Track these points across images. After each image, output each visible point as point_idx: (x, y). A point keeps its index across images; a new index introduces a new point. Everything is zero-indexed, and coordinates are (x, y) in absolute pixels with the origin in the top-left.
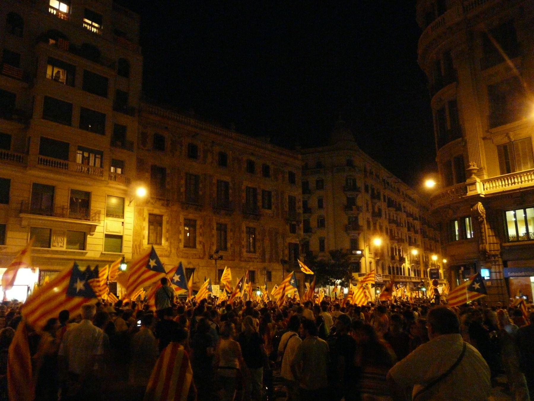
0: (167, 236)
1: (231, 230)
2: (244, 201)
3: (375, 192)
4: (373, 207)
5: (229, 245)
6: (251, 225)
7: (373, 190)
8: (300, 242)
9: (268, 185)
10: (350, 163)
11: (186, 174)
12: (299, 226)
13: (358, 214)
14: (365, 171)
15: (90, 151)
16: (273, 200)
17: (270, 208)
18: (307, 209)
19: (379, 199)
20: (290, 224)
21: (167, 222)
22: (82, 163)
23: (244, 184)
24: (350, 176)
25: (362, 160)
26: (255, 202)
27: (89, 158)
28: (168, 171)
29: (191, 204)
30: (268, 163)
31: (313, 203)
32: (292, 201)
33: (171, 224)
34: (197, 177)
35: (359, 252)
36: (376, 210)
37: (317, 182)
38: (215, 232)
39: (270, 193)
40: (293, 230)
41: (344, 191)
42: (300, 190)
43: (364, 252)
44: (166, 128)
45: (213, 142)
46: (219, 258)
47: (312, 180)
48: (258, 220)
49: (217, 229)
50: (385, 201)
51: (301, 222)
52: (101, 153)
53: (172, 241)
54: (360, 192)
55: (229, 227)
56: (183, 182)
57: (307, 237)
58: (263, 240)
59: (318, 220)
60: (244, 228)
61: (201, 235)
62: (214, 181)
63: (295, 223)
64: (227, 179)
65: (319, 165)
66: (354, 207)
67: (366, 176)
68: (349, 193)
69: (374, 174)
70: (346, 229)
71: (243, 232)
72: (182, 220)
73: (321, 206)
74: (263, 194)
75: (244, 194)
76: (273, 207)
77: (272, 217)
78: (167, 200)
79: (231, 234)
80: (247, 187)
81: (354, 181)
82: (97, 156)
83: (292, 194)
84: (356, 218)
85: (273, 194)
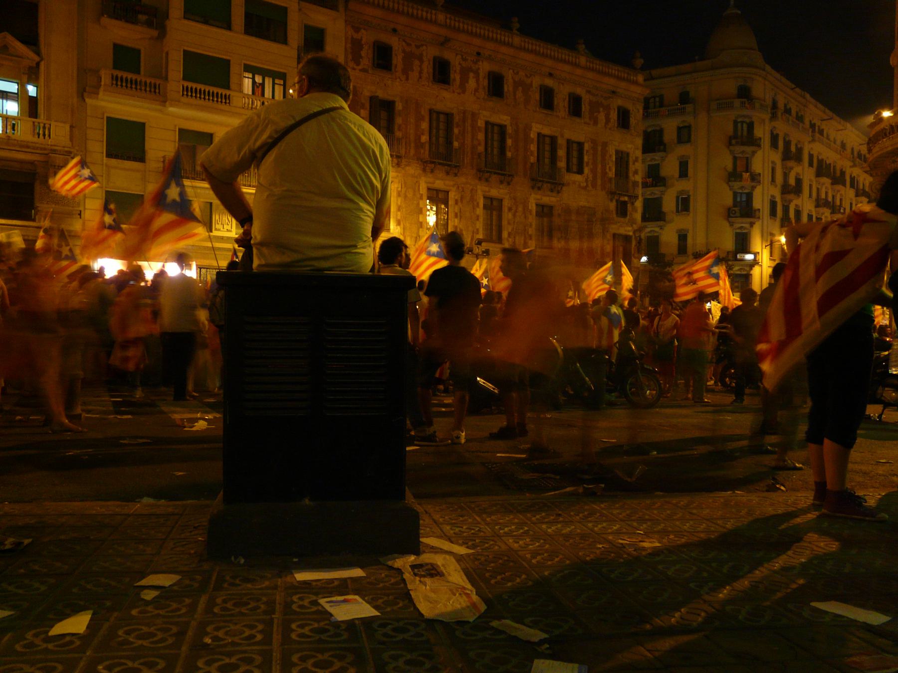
0: (399, 217)
2: (533, 159)
3: (793, 149)
4: (786, 176)
5: (505, 234)
7: (787, 144)
8: (634, 232)
9: (578, 131)
10: (744, 93)
11: (431, 111)
12: (633, 204)
13: (753, 188)
14: (775, 106)
15: (265, 73)
16: (586, 158)
17: (580, 171)
18: (655, 177)
19: (798, 158)
20: (617, 201)
21: (399, 195)
22: (253, 93)
23: (534, 129)
24: (744, 116)
25: (767, 85)
26: (554, 159)
27: (263, 85)
28: (399, 106)
29: (440, 164)
30: (579, 91)
31: (670, 168)
32: (622, 160)
33: (406, 197)
34: (449, 116)
35: (749, 257)
36: (792, 181)
37: (679, 129)
38: (480, 211)
39: (580, 145)
40: (622, 210)
41: (730, 144)
42: (639, 142)
43: (759, 257)
44: (395, 30)
45: (478, 54)
46: (483, 252)
47: (670, 126)
48: (558, 192)
49: (485, 207)
50: (811, 165)
51: (636, 197)
52: (283, 76)
53: (408, 225)
54: (759, 146)
55: (506, 203)
56: (425, 125)
57: (657, 229)
59: (677, 198)
60: (532, 207)
61: (456, 216)
62: (481, 123)
63: (626, 199)
65: (685, 98)
66: (746, 175)
67: (774, 117)
68: (738, 149)
69: (794, 112)
70: (729, 214)
72: (423, 190)
73: (684, 173)
74: (568, 148)
75: (533, 147)
77: (585, 188)
78: (398, 157)
79: (510, 215)
80: (539, 134)
81: (751, 126)
82: (277, 81)
84: (750, 196)
85: (586, 146)
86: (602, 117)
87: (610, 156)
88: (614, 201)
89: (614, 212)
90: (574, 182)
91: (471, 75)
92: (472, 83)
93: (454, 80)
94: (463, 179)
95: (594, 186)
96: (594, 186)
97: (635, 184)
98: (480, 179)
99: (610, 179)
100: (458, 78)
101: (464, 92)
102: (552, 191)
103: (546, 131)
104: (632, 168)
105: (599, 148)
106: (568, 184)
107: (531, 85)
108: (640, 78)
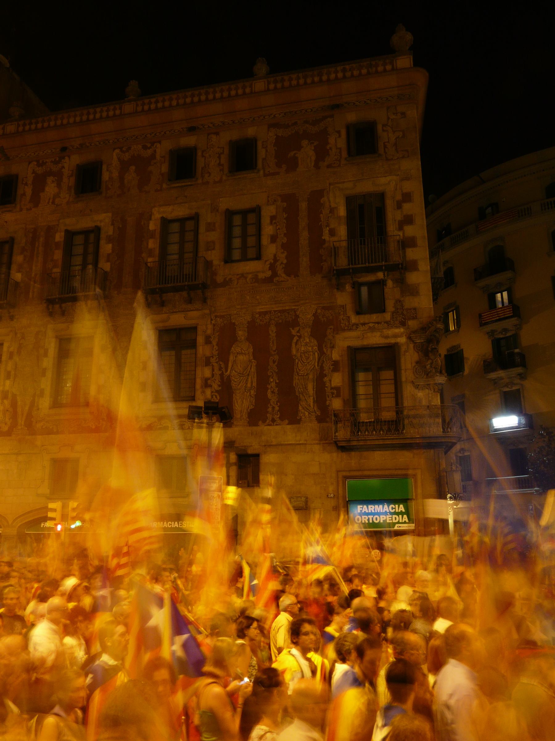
9: (258, 191)
12: (401, 282)
16: (268, 230)
20: (357, 286)
30: (251, 132)
39: (257, 210)
58: (224, 356)
62: (59, 237)
63: (380, 275)
64: (103, 219)
74: (229, 226)
76: (270, 250)
77: (269, 280)
85: (268, 212)
86: (307, 153)
87: (332, 210)
88: (348, 288)
90: (243, 276)
91: (50, 180)
92: (51, 189)
93: (24, 194)
95: (292, 269)
96: (292, 269)
97: (407, 243)
98: (51, 314)
99: (335, 252)
100: (29, 191)
101: (36, 205)
102: (190, 301)
103: (181, 211)
104: (393, 216)
105: (303, 205)
106: (226, 283)
107: (153, 156)
108: (404, 62)
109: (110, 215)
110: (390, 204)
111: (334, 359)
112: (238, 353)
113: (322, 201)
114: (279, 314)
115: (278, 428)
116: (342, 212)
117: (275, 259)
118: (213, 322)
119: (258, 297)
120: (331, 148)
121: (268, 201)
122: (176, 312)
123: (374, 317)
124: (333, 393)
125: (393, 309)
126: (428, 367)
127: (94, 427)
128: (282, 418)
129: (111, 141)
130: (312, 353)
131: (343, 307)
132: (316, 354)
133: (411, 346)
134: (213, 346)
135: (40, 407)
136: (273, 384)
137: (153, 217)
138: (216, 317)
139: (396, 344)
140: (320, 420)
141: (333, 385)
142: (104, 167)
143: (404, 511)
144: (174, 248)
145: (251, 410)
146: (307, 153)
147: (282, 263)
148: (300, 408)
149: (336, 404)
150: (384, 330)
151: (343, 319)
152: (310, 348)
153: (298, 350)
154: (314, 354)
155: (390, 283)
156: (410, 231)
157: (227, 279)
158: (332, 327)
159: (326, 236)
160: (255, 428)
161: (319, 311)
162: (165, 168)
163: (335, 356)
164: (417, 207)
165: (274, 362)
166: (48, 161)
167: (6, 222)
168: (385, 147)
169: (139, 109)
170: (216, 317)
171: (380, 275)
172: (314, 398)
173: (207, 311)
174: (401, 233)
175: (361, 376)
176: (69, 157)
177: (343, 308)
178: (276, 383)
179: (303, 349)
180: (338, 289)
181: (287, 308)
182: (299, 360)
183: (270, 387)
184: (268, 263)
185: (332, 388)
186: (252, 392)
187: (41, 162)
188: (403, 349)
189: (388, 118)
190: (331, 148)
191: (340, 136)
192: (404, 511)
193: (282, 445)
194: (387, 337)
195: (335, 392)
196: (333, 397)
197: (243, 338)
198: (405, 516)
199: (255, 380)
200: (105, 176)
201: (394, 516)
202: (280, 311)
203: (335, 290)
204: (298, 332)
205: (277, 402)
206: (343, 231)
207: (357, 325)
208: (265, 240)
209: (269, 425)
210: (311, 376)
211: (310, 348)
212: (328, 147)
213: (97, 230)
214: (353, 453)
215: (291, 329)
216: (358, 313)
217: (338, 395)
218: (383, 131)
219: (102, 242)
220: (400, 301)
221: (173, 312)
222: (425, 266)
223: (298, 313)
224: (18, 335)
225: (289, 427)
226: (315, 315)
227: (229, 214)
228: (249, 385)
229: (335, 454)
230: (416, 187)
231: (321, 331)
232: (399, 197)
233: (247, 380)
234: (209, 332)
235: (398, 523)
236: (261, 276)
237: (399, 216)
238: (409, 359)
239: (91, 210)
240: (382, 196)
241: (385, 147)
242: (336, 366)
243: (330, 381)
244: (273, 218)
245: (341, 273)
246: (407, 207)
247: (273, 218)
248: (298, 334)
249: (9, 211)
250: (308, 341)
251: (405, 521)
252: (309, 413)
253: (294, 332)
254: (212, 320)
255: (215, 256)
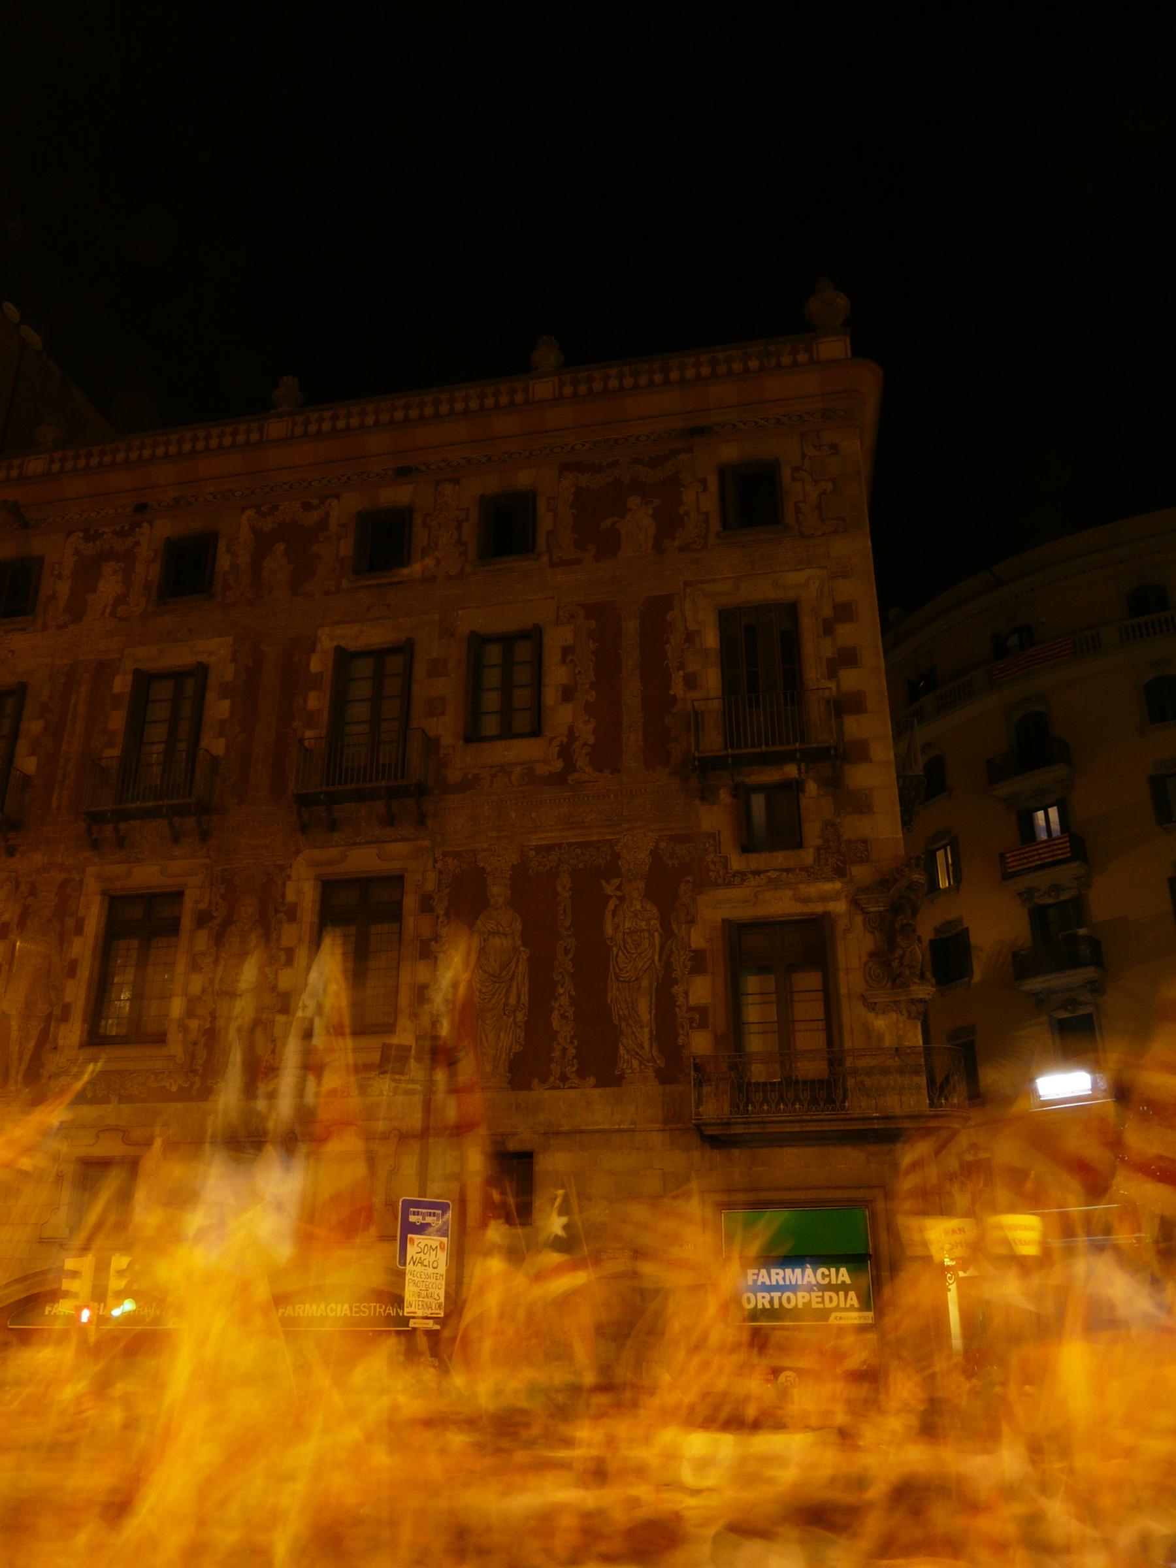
1: (202, 919)
5: (177, 1007)
6: (363, 860)
12: (834, 784)
16: (557, 675)
20: (742, 793)
30: (524, 478)
39: (534, 635)
62: (121, 684)
63: (791, 770)
64: (214, 650)
71: (292, 914)
74: (476, 667)
76: (562, 717)
77: (558, 779)
83: (759, 590)
85: (556, 639)
86: (639, 521)
87: (690, 637)
88: (724, 796)
89: (726, 836)
92: (109, 587)
94: (38, 859)
95: (606, 755)
96: (606, 755)
97: (846, 705)
98: (95, 845)
100: (64, 589)
102: (390, 820)
103: (375, 636)
104: (815, 649)
108: (834, 347)
109: (229, 640)
110: (808, 623)
111: (694, 946)
112: (489, 933)
113: (669, 617)
114: (579, 851)
115: (572, 1094)
116: (711, 640)
117: (572, 736)
118: (438, 866)
119: (534, 815)
120: (687, 514)
121: (558, 616)
122: (360, 844)
123: (780, 858)
124: (691, 1020)
125: (819, 842)
126: (895, 964)
127: (174, 1089)
128: (582, 1074)
129: (238, 494)
130: (646, 935)
131: (712, 836)
132: (656, 934)
133: (859, 919)
134: (438, 918)
135: (61, 1042)
136: (564, 1000)
137: (318, 646)
138: (445, 854)
139: (826, 915)
140: (665, 1077)
141: (692, 1002)
142: (222, 545)
143: (848, 1281)
144: (359, 711)
145: (515, 1054)
146: (639, 521)
147: (585, 744)
148: (622, 1051)
149: (700, 1043)
150: (801, 886)
151: (713, 862)
152: (643, 924)
153: (616, 928)
154: (652, 935)
155: (811, 787)
156: (850, 679)
157: (470, 776)
158: (690, 878)
159: (678, 688)
160: (523, 1094)
161: (663, 845)
162: (346, 548)
163: (697, 939)
164: (864, 632)
165: (567, 952)
166: (106, 530)
167: (12, 652)
168: (798, 511)
169: (299, 430)
170: (445, 854)
171: (791, 770)
172: (651, 1032)
173: (426, 843)
174: (832, 685)
175: (752, 983)
176: (150, 522)
177: (714, 839)
178: (570, 996)
179: (627, 925)
180: (702, 798)
181: (595, 838)
182: (620, 949)
183: (556, 1005)
184: (556, 743)
185: (690, 1009)
186: (520, 1017)
187: (92, 532)
188: (841, 925)
189: (804, 455)
190: (687, 514)
191: (705, 490)
192: (848, 1281)
193: (581, 1132)
194: (806, 901)
195: (697, 1016)
196: (691, 1027)
197: (501, 900)
198: (852, 1294)
199: (525, 989)
200: (224, 562)
201: (827, 1294)
202: (580, 845)
203: (697, 801)
204: (618, 888)
205: (572, 1037)
206: (712, 679)
207: (742, 875)
208: (550, 696)
209: (553, 1088)
210: (645, 983)
211: (643, 924)
212: (681, 511)
213: (201, 671)
214: (736, 1152)
215: (603, 882)
216: (747, 847)
217: (703, 1025)
218: (794, 479)
219: (210, 697)
220: (833, 825)
221: (355, 844)
222: (883, 752)
223: (618, 848)
224: (23, 888)
225: (597, 1091)
226: (652, 853)
227: (477, 642)
228: (512, 1001)
229: (696, 1154)
230: (862, 592)
231: (668, 886)
232: (827, 612)
233: (508, 991)
234: (430, 886)
235: (837, 1308)
236: (541, 770)
237: (828, 651)
238: (853, 949)
239: (190, 630)
240: (792, 609)
241: (798, 511)
242: (698, 963)
243: (686, 993)
244: (566, 651)
245: (708, 766)
246: (844, 631)
247: (566, 651)
248: (619, 894)
249: (23, 630)
250: (639, 907)
251: (852, 1306)
252: (641, 1063)
253: (609, 889)
254: (435, 861)
255: (446, 728)
